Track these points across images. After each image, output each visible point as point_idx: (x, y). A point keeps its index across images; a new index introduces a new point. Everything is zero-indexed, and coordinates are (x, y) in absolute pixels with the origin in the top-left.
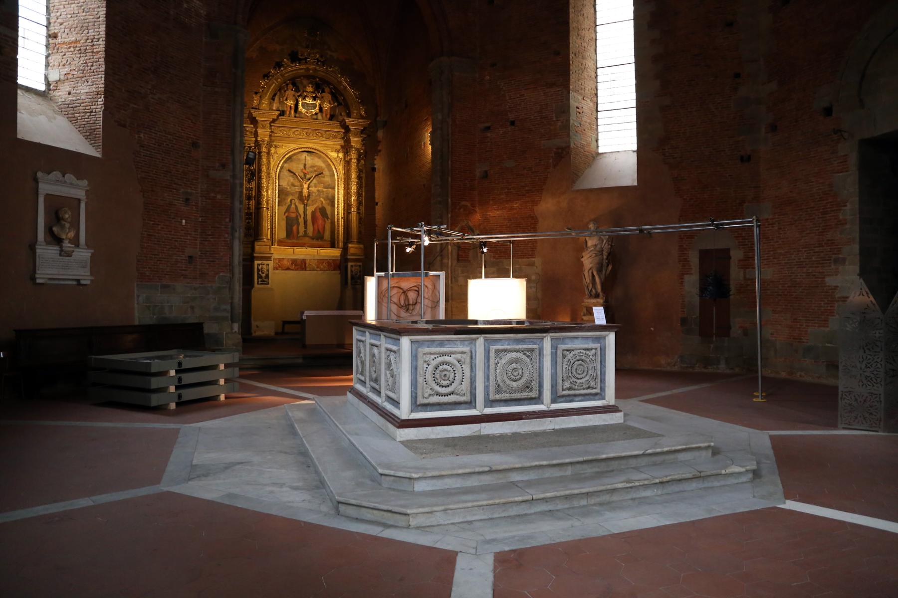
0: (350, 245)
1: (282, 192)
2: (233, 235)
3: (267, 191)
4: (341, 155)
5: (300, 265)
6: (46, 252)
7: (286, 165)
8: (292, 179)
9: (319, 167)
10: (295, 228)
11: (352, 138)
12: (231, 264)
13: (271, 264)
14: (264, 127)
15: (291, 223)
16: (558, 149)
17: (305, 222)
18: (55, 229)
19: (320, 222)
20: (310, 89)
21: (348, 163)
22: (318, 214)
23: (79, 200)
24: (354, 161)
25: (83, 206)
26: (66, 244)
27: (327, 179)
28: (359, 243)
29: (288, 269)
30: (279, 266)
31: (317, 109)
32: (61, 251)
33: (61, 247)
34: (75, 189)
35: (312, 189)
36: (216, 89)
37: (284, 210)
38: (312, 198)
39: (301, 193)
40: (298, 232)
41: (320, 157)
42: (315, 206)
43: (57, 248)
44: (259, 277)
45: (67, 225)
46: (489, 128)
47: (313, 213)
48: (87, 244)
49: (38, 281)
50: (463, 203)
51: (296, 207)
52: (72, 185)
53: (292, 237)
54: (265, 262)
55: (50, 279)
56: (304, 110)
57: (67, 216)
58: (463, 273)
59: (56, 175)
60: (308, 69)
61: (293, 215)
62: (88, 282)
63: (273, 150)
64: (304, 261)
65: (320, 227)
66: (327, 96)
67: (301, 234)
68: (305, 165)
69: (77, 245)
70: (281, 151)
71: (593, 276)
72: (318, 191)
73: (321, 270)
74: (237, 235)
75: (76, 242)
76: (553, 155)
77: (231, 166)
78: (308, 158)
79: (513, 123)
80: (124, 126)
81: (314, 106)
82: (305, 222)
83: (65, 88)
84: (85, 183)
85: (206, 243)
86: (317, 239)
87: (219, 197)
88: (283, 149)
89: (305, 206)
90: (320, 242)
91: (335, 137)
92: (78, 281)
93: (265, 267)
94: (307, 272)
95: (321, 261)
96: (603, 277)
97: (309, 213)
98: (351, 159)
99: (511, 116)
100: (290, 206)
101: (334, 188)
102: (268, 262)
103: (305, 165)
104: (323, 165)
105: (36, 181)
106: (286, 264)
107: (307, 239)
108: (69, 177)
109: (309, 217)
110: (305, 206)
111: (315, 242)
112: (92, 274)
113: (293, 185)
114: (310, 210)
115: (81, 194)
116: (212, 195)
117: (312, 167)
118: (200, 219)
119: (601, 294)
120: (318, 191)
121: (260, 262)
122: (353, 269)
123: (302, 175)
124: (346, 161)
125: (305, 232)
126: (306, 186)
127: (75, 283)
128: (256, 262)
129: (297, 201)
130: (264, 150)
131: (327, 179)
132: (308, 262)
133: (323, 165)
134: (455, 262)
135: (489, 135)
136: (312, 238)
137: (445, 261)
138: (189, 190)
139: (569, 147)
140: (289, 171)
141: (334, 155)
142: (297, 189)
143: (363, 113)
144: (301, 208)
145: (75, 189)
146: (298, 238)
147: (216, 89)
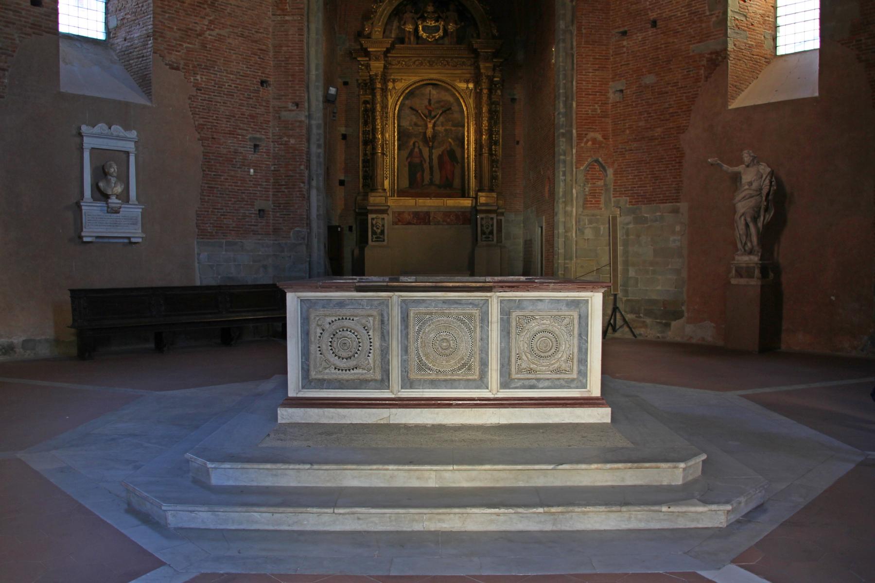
0: (480, 194)
1: (403, 135)
2: (309, 183)
3: (383, 134)
4: (471, 86)
5: (423, 218)
6: (91, 209)
7: (407, 102)
8: (414, 119)
10: (418, 175)
11: (481, 66)
12: (308, 218)
13: (388, 218)
16: (711, 53)
17: (431, 168)
18: (101, 184)
21: (478, 96)
23: (127, 153)
24: (485, 91)
25: (132, 159)
26: (113, 200)
27: (457, 115)
28: (491, 190)
29: (409, 223)
30: (399, 219)
32: (108, 207)
33: (107, 204)
34: (124, 140)
35: (439, 128)
36: (287, 18)
37: (406, 155)
39: (425, 133)
40: (423, 181)
41: (447, 90)
43: (103, 204)
44: (374, 233)
45: (113, 180)
46: (624, 33)
47: (440, 157)
48: (138, 199)
49: (85, 239)
50: (592, 135)
51: (420, 151)
52: (119, 138)
53: (414, 185)
55: (97, 237)
56: (425, 35)
57: (112, 170)
59: (101, 127)
61: (417, 160)
62: (140, 240)
63: (390, 85)
64: (428, 214)
68: (430, 100)
69: (127, 200)
71: (747, 225)
72: (446, 130)
73: (448, 224)
74: (314, 183)
75: (125, 197)
76: (704, 62)
77: (306, 105)
78: (434, 92)
79: (654, 24)
80: (177, 69)
82: (431, 168)
83: (122, 34)
84: (133, 134)
85: (280, 194)
87: (292, 141)
88: (401, 83)
89: (431, 148)
91: (463, 64)
92: (129, 238)
93: (380, 221)
96: (760, 225)
97: (435, 157)
98: (481, 90)
99: (653, 15)
100: (412, 151)
102: (385, 216)
103: (430, 100)
104: (451, 99)
105: (80, 135)
106: (407, 217)
108: (117, 129)
110: (431, 148)
112: (143, 232)
114: (436, 153)
115: (130, 146)
116: (285, 139)
117: (438, 102)
118: (272, 168)
119: (756, 248)
120: (446, 130)
121: (374, 216)
122: (484, 222)
123: (426, 112)
124: (476, 93)
125: (431, 179)
126: (430, 125)
127: (126, 241)
128: (370, 216)
129: (421, 144)
130: (379, 86)
131: (457, 115)
132: (432, 215)
133: (451, 99)
134: (581, 209)
135: (625, 43)
137: (568, 208)
138: (258, 135)
139: (726, 49)
140: (411, 108)
141: (463, 85)
142: (421, 130)
144: (426, 152)
145: (124, 140)
147: (287, 18)
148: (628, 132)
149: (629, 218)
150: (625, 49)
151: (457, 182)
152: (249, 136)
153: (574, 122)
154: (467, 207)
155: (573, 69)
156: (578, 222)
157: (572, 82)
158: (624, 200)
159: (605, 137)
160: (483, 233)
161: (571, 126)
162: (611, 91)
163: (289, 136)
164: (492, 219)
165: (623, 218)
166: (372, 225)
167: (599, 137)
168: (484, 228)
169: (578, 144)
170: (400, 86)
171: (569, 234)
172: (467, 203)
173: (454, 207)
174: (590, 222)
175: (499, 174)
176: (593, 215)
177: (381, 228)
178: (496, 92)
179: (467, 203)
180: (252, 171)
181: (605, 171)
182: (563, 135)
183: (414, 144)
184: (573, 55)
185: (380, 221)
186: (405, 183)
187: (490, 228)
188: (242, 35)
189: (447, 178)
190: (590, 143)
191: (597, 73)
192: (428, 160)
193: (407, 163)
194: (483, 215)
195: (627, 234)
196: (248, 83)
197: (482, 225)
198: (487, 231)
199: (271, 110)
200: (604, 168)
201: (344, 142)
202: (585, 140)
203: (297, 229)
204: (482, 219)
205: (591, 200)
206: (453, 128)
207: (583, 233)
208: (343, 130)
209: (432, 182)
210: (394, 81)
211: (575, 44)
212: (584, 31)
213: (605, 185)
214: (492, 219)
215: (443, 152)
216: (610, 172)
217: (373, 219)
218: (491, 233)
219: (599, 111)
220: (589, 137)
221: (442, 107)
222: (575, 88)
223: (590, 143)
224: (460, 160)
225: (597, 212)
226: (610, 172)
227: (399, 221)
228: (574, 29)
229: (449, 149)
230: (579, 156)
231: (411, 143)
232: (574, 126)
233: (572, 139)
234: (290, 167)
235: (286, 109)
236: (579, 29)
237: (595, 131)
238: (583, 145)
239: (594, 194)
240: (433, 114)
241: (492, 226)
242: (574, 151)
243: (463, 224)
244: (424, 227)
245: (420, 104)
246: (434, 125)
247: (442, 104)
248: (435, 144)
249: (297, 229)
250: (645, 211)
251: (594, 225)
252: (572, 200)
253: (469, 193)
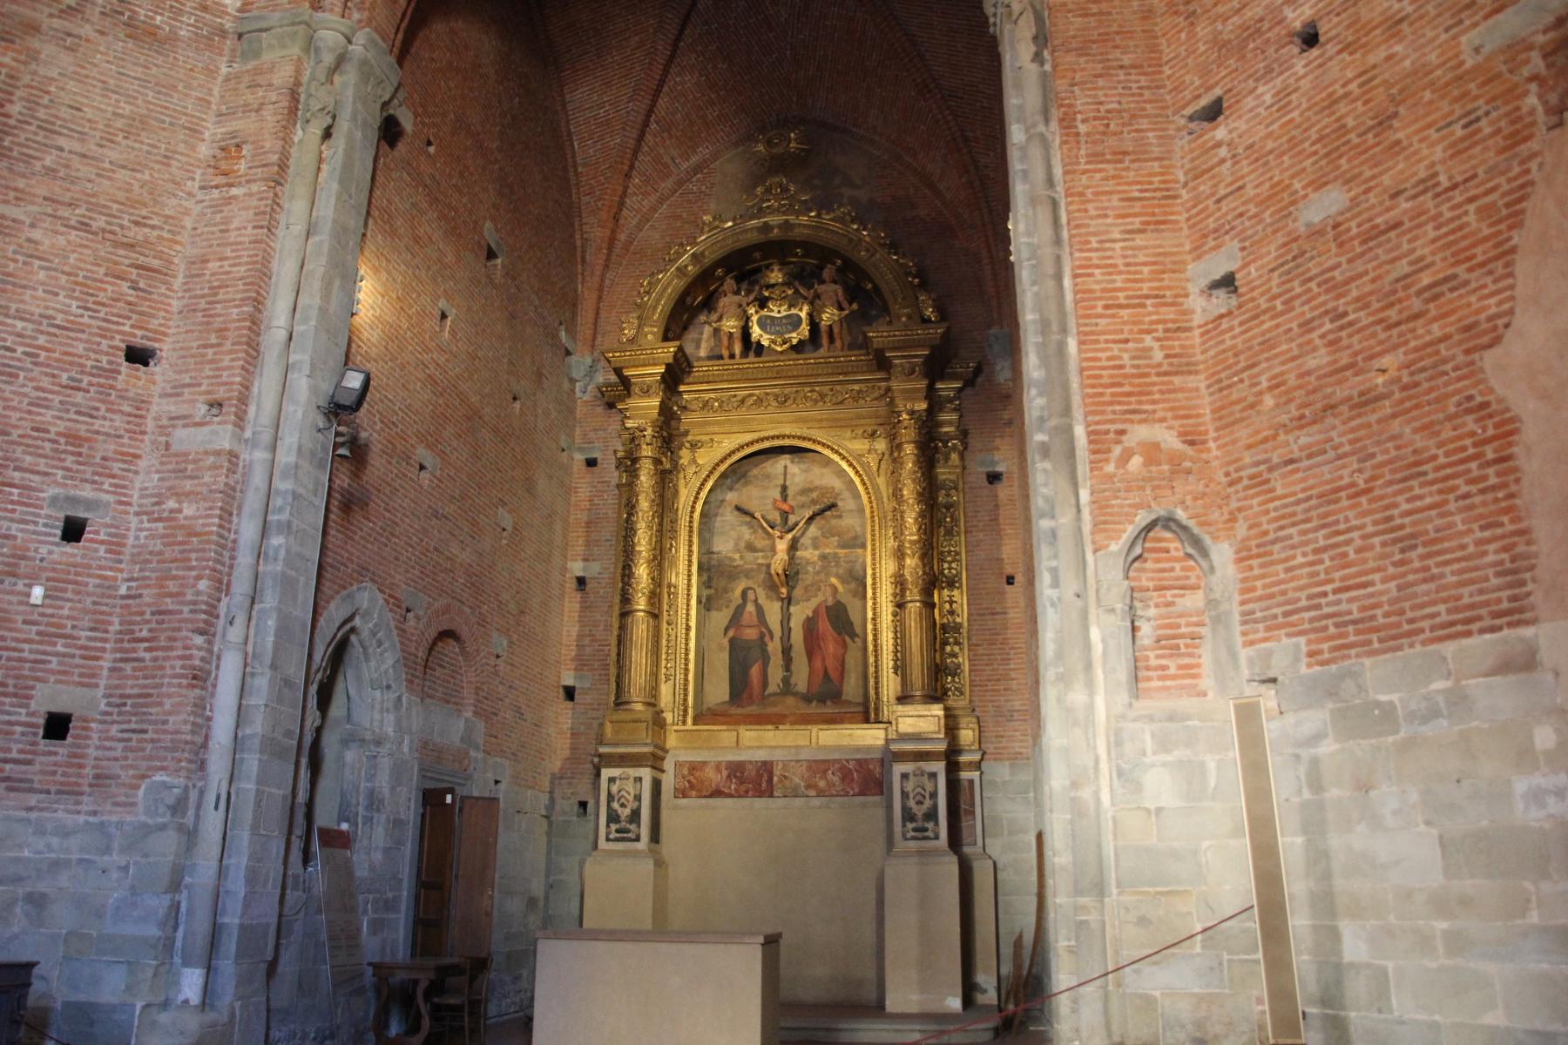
5: (755, 781)
8: (746, 534)
9: (824, 491)
10: (755, 671)
14: (646, 392)
15: (744, 658)
17: (787, 651)
19: (830, 647)
20: (776, 276)
22: (824, 626)
27: (849, 522)
29: (717, 793)
31: (805, 329)
37: (725, 622)
38: (807, 579)
40: (765, 684)
42: (814, 602)
44: (613, 817)
47: (810, 626)
50: (1140, 433)
51: (760, 610)
54: (633, 772)
58: (1164, 745)
60: (766, 227)
61: (751, 634)
64: (766, 767)
65: (831, 664)
66: (831, 290)
67: (773, 688)
68: (784, 488)
70: (706, 458)
72: (823, 557)
73: (821, 793)
79: (1310, 39)
81: (795, 323)
82: (787, 651)
85: (128, 667)
86: (822, 701)
87: (189, 510)
90: (829, 709)
94: (777, 803)
95: (819, 767)
97: (796, 623)
100: (740, 610)
101: (864, 546)
103: (784, 488)
104: (837, 483)
106: (714, 777)
107: (790, 700)
109: (797, 637)
110: (789, 601)
111: (814, 709)
113: (751, 548)
114: (799, 614)
117: (805, 491)
118: (123, 591)
120: (823, 557)
121: (615, 772)
122: (909, 786)
123: (775, 516)
125: (786, 681)
126: (782, 546)
132: (777, 772)
134: (1123, 697)
136: (807, 699)
138: (87, 492)
140: (738, 509)
143: (929, 312)
146: (763, 698)
148: (1269, 401)
149: (1316, 718)
150: (1223, 152)
151: (851, 689)
152: (52, 491)
153: (1076, 400)
154: (869, 749)
155: (1058, 241)
156: (1117, 742)
157: (1058, 277)
158: (1286, 652)
159: (1192, 439)
160: (908, 816)
161: (1067, 411)
162: (1193, 289)
163: (180, 496)
164: (933, 776)
165: (1290, 719)
166: (610, 797)
167: (1169, 439)
168: (912, 803)
169: (1095, 466)
170: (706, 458)
171: (1085, 794)
172: (871, 737)
173: (839, 748)
174: (1164, 745)
175: (963, 660)
176: (1171, 718)
177: (632, 805)
178: (947, 459)
179: (871, 737)
180: (38, 593)
181: (1204, 553)
182: (1045, 451)
183: (744, 594)
184: (1055, 204)
185: (630, 787)
186: (719, 691)
187: (928, 803)
188: (84, 226)
189: (826, 673)
190: (1136, 462)
191: (1139, 241)
192: (777, 633)
193: (726, 642)
194: (908, 767)
195: (1316, 781)
196: (80, 348)
197: (904, 795)
198: (920, 811)
199: (150, 425)
200: (1196, 542)
201: (579, 595)
202: (1117, 450)
203: (159, 777)
204: (905, 776)
205: (1157, 661)
206: (842, 552)
207: (1138, 788)
208: (577, 568)
209: (787, 688)
210: (694, 446)
211: (1058, 171)
212: (1082, 128)
213: (1212, 603)
214: (933, 776)
215: (816, 612)
216: (1222, 554)
217: (612, 780)
218: (932, 815)
219: (1158, 356)
220: (1130, 440)
221: (814, 502)
222: (1069, 297)
223: (1136, 462)
224: (858, 630)
225: (1186, 704)
226: (1222, 554)
227: (692, 787)
228: (1054, 130)
229: (830, 602)
230: (1099, 504)
231: (738, 592)
232: (1078, 413)
233: (1071, 453)
234: (172, 586)
235: (186, 420)
236: (1067, 122)
237: (1149, 419)
238: (1110, 468)
239: (1169, 642)
240: (792, 519)
241: (934, 795)
242: (1085, 495)
243: (862, 793)
244: (760, 803)
245: (760, 495)
246: (793, 546)
247: (814, 495)
248: (797, 592)
249: (159, 777)
250: (1380, 678)
251: (1179, 753)
252: (1089, 667)
253: (877, 714)
